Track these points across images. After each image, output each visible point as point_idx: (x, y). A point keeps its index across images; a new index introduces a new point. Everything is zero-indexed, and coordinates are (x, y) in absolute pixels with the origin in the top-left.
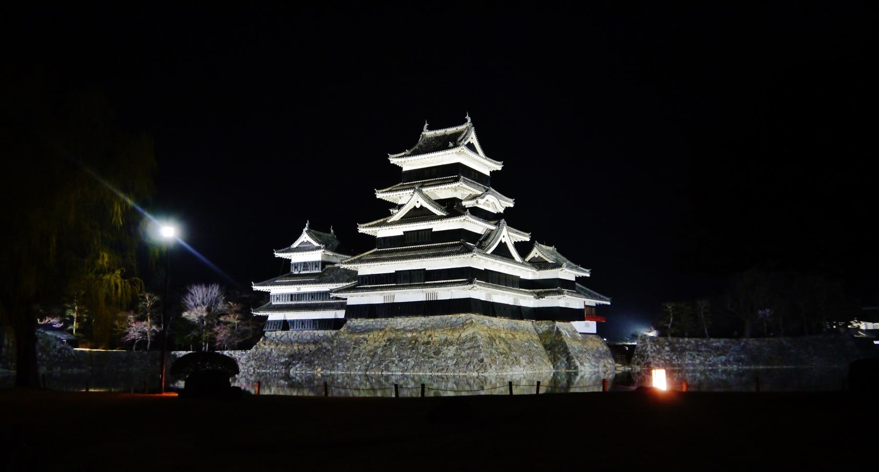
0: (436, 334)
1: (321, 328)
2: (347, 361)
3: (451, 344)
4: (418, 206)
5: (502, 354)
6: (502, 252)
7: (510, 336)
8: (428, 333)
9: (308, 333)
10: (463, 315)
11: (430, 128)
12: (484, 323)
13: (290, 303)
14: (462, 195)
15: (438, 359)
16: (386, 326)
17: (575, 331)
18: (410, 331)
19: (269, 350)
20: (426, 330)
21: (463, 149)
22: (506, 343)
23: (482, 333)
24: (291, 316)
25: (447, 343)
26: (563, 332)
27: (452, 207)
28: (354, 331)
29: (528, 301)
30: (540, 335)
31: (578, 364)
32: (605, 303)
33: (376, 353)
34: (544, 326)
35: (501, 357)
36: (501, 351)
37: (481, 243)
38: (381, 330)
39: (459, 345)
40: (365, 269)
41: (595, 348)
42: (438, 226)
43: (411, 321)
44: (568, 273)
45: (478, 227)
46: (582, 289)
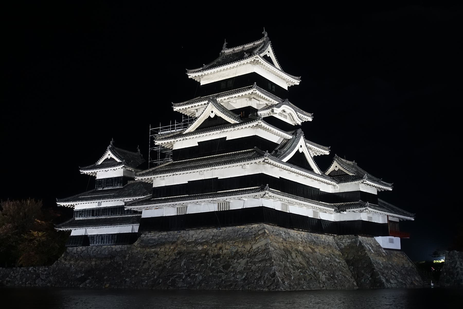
0: (227, 247)
1: (117, 243)
2: (136, 276)
3: (242, 256)
4: (212, 116)
5: (298, 268)
6: (299, 161)
7: (309, 249)
8: (219, 246)
9: (107, 247)
10: (256, 225)
11: (229, 47)
12: (279, 235)
13: (91, 218)
14: (258, 105)
15: (226, 274)
16: (178, 239)
17: (379, 246)
18: (202, 244)
19: (68, 266)
20: (217, 242)
21: (258, 58)
22: (304, 257)
23: (275, 244)
24: (92, 231)
25: (237, 255)
26: (367, 246)
27: (246, 115)
28: (147, 244)
29: (329, 215)
30: (341, 250)
31: (384, 280)
32: (409, 218)
33: (165, 267)
34: (346, 240)
35: (297, 272)
36: (298, 265)
37: (276, 151)
38: (173, 243)
39: (250, 257)
40: (161, 181)
41: (401, 265)
42: (231, 134)
43: (203, 234)
44: (368, 187)
45: (274, 136)
46: (385, 205)
